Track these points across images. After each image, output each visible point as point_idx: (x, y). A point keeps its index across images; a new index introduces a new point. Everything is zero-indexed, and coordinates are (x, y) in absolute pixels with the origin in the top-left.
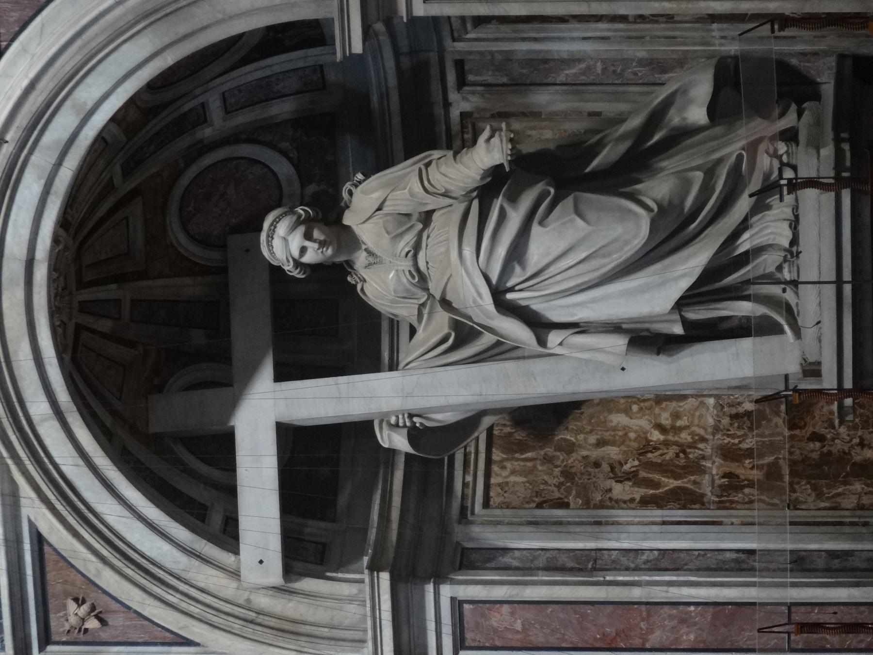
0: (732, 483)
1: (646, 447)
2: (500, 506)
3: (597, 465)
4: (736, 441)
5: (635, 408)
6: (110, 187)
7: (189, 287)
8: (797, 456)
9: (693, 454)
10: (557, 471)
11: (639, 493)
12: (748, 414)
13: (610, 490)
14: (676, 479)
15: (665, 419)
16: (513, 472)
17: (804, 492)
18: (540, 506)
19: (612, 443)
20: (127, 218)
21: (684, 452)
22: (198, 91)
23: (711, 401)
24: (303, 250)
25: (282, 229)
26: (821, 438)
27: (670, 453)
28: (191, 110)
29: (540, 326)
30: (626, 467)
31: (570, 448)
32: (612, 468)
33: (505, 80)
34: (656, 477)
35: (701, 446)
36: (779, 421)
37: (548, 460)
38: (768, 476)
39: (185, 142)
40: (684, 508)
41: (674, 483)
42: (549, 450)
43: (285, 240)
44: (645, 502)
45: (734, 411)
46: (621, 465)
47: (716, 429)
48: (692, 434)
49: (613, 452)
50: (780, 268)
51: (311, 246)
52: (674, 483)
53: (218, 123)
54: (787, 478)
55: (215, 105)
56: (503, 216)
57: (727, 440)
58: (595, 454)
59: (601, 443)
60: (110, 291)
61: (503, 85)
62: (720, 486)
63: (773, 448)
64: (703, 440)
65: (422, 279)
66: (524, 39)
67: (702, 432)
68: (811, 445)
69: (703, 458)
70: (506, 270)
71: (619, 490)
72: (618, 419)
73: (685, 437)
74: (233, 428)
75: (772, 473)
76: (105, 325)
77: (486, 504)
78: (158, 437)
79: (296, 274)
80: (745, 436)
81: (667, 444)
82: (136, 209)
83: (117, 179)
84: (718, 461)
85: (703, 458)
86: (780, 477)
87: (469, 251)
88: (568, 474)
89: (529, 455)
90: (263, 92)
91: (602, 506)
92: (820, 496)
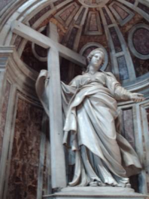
0: (17, 167)
1: (28, 145)
2: (18, 101)
3: (25, 130)
4: (27, 170)
5: (37, 144)
6: (109, 22)
7: (76, 46)
8: (22, 188)
9: (25, 157)
10: (24, 119)
11: (17, 138)
12: (33, 175)
13: (19, 131)
14: (20, 150)
15: (34, 152)
16: (25, 108)
17: (12, 188)
18: (17, 111)
19: (30, 136)
20: (97, 30)
21: (25, 155)
22: (127, 48)
23: (37, 165)
24: (97, 57)
25: (102, 53)
26: (25, 196)
27: (25, 151)
28: (121, 48)
29: (78, 108)
30: (23, 138)
31: (30, 125)
32: (24, 134)
33: (125, 119)
34: (20, 145)
35: (26, 160)
36: (30, 184)
37: (27, 118)
38: (17, 178)
39: (112, 47)
40: (13, 150)
41: (18, 149)
42: (29, 119)
43: (99, 53)
44: (15, 139)
45: (35, 171)
46: (24, 136)
47: (30, 165)
48: (30, 158)
49: (28, 135)
50: (95, 180)
51: (98, 58)
52: (18, 149)
53: (114, 54)
54: (16, 183)
55: (121, 54)
56: (111, 101)
57: (27, 168)
58: (28, 131)
59: (30, 133)
60: (83, 23)
61: (123, 119)
62: (16, 163)
63: (24, 181)
64: (28, 161)
65: (89, 83)
66: (142, 122)
67: (30, 161)
68: (24, 193)
69: (24, 160)
70: (97, 99)
71: (18, 133)
72: (35, 139)
73: (29, 156)
74: (50, 38)
75: (18, 179)
76: (76, 18)
77: (19, 98)
78: (48, 24)
79: (89, 56)
80: (27, 173)
81: (28, 150)
82: (99, 33)
83: (111, 26)
84: (22, 164)
85: (24, 160)
86: (16, 181)
87: (101, 91)
88: (23, 122)
89: (29, 115)
90: (122, 64)
91: (15, 127)
92: (11, 193)
